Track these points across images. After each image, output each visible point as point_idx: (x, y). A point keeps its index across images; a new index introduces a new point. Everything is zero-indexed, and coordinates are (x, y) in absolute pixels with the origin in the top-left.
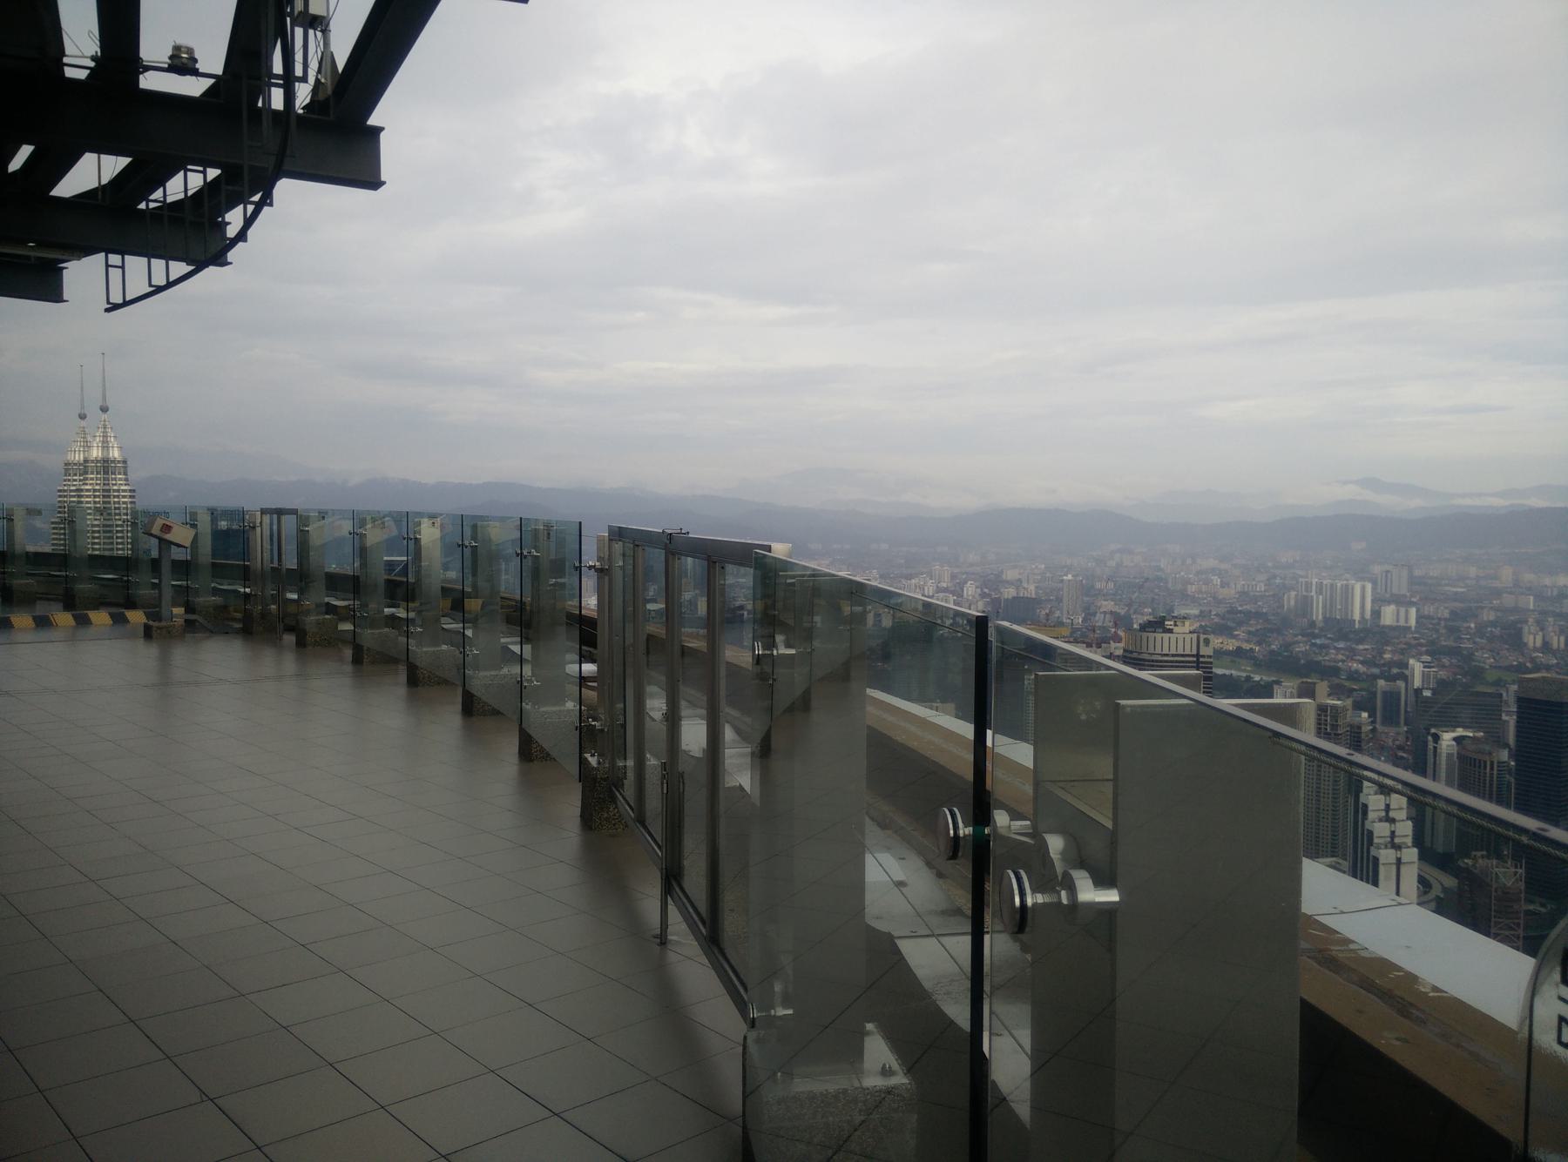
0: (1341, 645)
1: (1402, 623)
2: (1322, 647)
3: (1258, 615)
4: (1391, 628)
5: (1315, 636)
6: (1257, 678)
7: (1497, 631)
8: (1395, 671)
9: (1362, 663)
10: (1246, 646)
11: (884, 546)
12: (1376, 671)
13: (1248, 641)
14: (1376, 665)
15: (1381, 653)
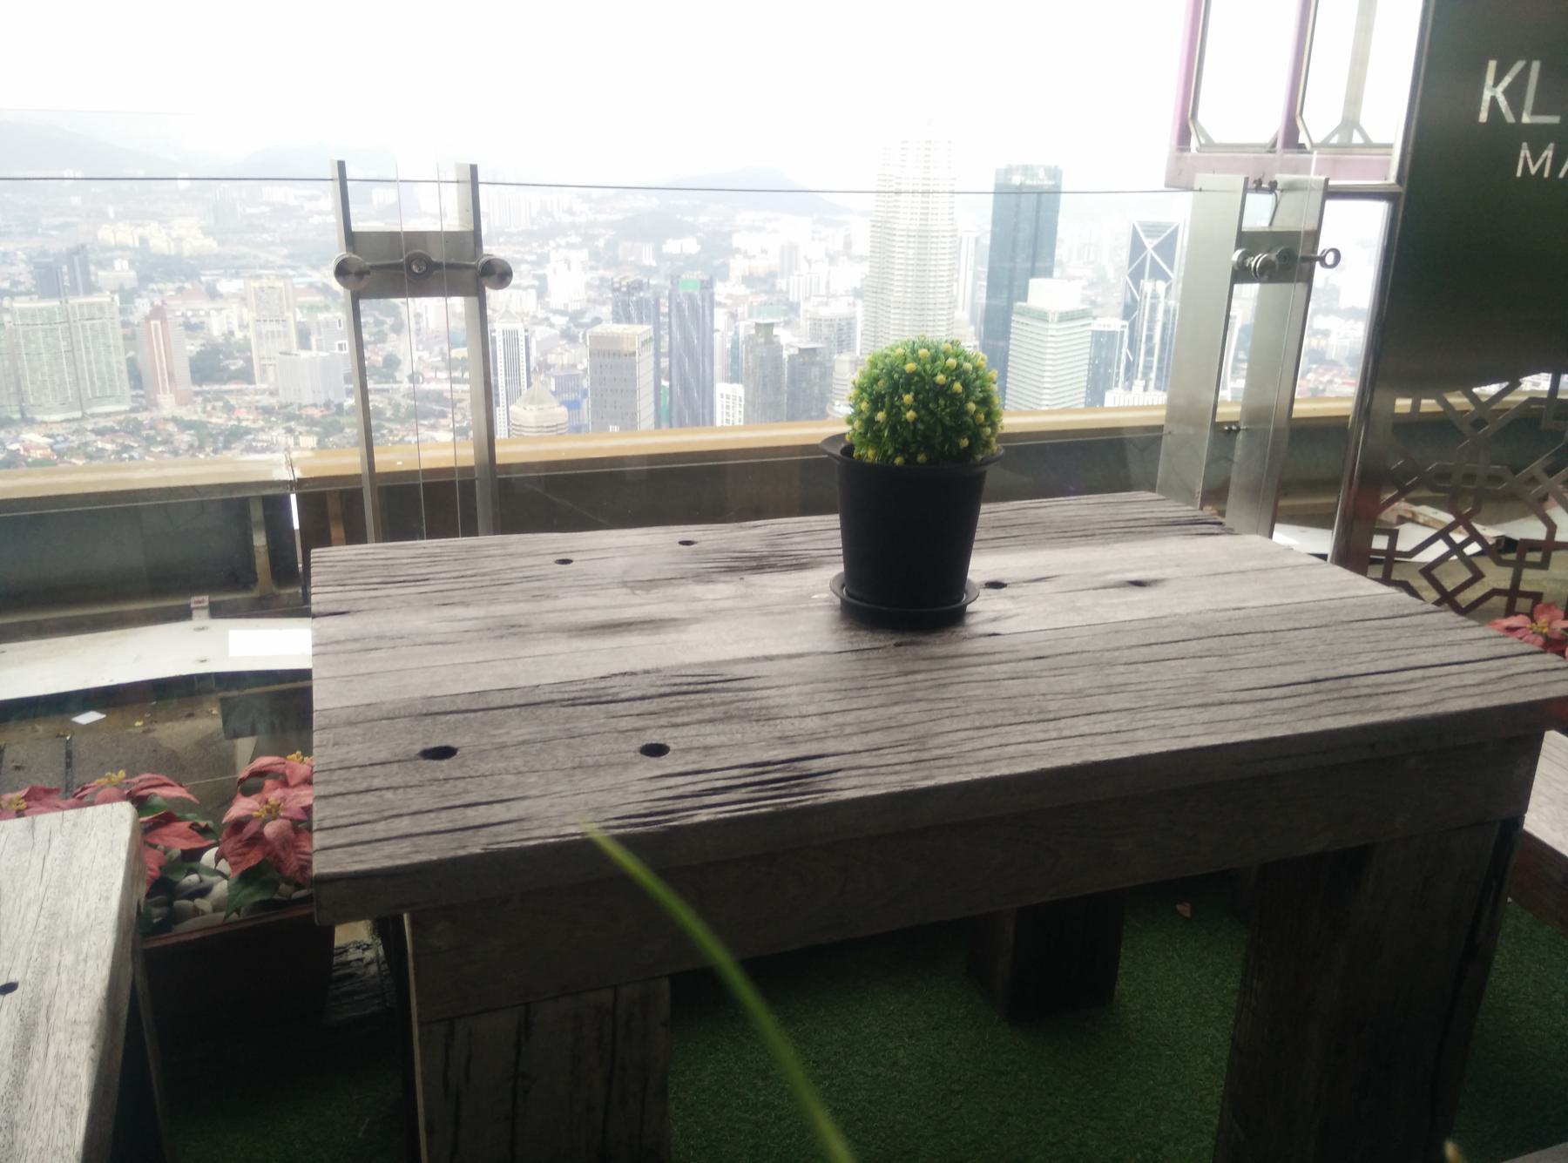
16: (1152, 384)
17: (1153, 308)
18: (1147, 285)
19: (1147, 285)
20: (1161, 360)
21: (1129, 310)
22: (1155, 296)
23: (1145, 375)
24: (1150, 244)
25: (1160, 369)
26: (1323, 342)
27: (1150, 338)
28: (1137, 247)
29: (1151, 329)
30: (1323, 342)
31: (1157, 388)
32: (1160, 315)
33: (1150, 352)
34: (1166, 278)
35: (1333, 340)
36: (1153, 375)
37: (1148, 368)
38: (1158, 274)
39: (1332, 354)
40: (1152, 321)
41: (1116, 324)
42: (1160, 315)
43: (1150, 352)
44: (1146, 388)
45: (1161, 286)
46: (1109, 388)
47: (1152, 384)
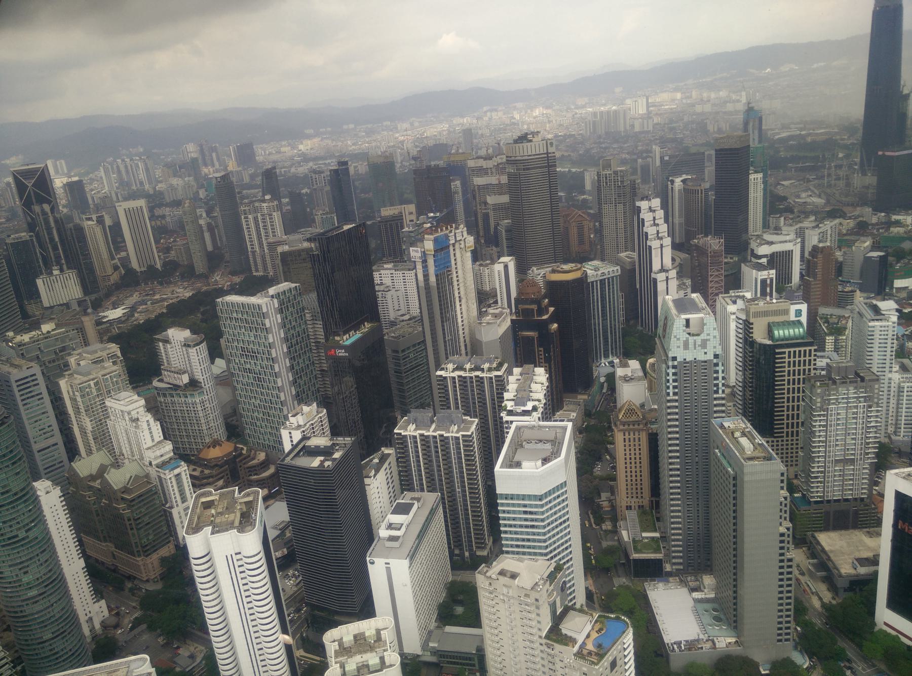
0: (615, 146)
1: (646, 129)
2: (606, 148)
3: (571, 136)
4: (640, 132)
5: (604, 143)
6: (574, 170)
7: (694, 126)
8: (645, 155)
9: (628, 153)
10: (566, 154)
11: (352, 126)
12: (635, 157)
13: (566, 151)
14: (635, 154)
15: (636, 147)
16: (65, 267)
17: (47, 222)
18: (37, 208)
19: (37, 208)
20: (64, 251)
21: (32, 227)
22: (44, 213)
23: (58, 263)
24: (30, 183)
25: (66, 257)
26: (163, 222)
27: (52, 239)
28: (21, 187)
29: (50, 233)
30: (163, 222)
31: (69, 268)
32: (53, 224)
33: (55, 248)
34: (49, 202)
35: (168, 219)
36: (63, 261)
37: (58, 258)
38: (41, 200)
39: (171, 227)
40: (49, 229)
41: (24, 235)
42: (53, 224)
43: (55, 248)
44: (62, 270)
45: (46, 207)
46: (37, 277)
47: (65, 267)
